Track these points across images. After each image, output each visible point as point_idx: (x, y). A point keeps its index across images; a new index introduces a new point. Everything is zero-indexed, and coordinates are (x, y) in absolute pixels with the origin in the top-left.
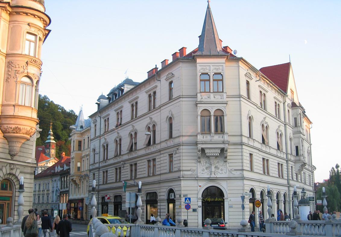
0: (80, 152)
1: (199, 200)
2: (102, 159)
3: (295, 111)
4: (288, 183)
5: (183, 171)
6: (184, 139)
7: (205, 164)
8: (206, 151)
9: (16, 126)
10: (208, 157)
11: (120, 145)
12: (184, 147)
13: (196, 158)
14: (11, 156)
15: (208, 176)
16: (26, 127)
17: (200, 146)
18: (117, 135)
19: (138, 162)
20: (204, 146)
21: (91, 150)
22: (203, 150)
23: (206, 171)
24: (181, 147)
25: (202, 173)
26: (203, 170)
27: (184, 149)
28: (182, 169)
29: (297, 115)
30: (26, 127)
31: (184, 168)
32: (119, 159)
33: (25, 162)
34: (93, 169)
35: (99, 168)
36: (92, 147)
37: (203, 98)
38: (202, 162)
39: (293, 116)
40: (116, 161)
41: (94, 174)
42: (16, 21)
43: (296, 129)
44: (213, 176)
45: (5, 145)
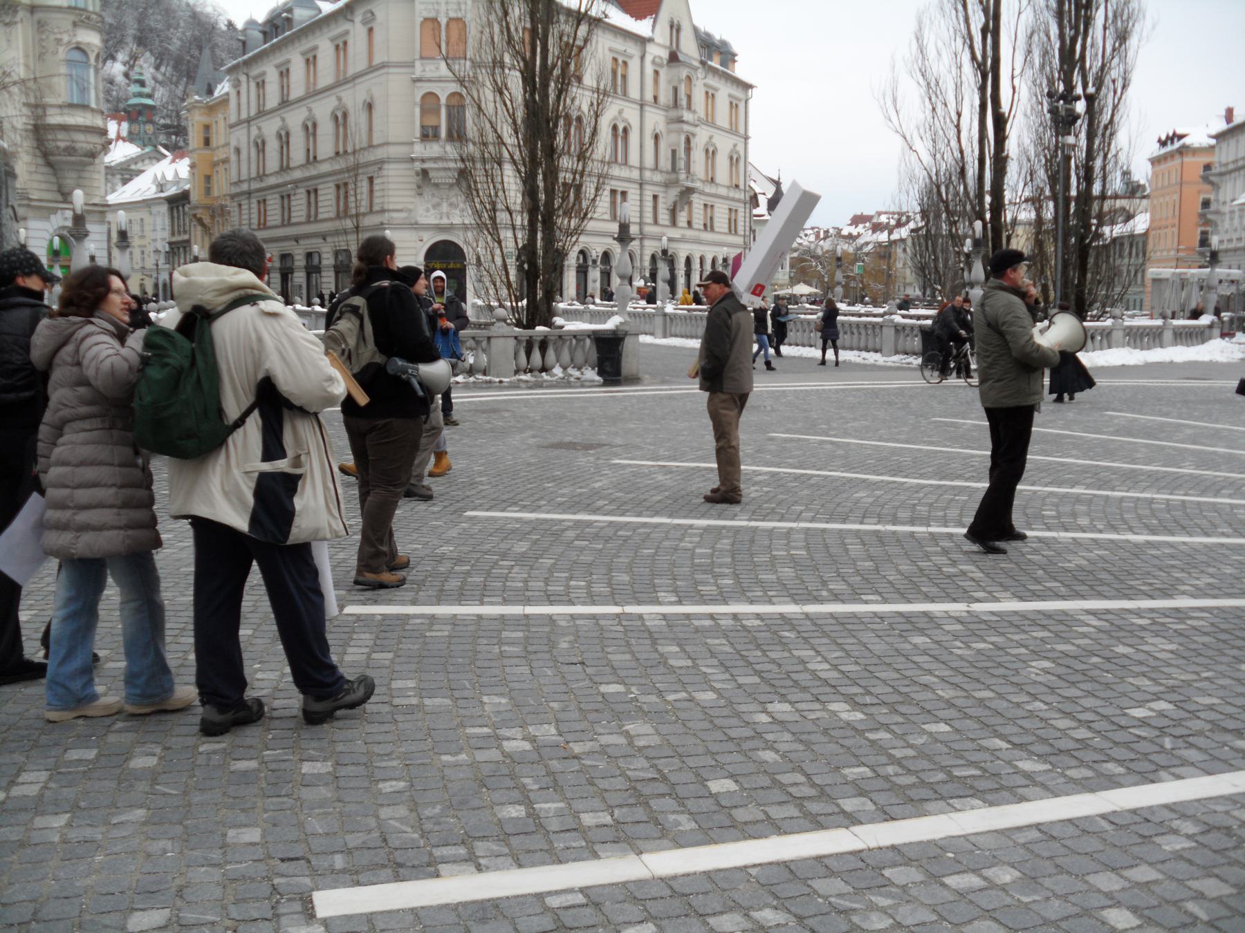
0: (208, 152)
2: (254, 175)
3: (675, 71)
4: (641, 229)
5: (389, 211)
6: (393, 151)
8: (431, 174)
10: (437, 185)
11: (288, 143)
12: (392, 166)
13: (414, 186)
15: (437, 222)
17: (418, 166)
18: (280, 123)
19: (320, 187)
20: (426, 166)
21: (232, 150)
22: (425, 172)
23: (432, 211)
24: (386, 166)
26: (428, 210)
27: (392, 170)
28: (386, 207)
29: (680, 81)
31: (391, 207)
32: (287, 177)
34: (237, 195)
35: (249, 194)
36: (233, 143)
38: (425, 195)
39: (669, 82)
40: (280, 180)
41: (240, 205)
43: (674, 114)
44: (445, 221)
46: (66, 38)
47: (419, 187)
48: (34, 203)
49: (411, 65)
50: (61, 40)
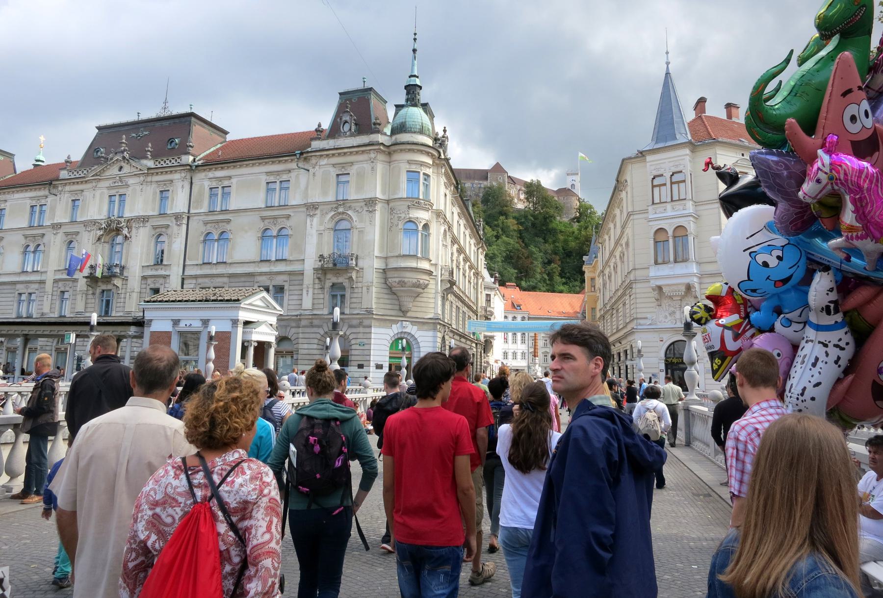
1: (660, 361)
7: (667, 307)
8: (664, 290)
9: (400, 279)
10: (671, 297)
14: (403, 312)
16: (411, 280)
17: (654, 283)
20: (659, 283)
22: (660, 288)
23: (669, 318)
25: (665, 322)
30: (411, 280)
33: (424, 318)
37: (657, 212)
42: (395, 161)
45: (394, 301)
46: (403, 216)
47: (657, 300)
48: (374, 317)
49: (645, 211)
50: (400, 217)
